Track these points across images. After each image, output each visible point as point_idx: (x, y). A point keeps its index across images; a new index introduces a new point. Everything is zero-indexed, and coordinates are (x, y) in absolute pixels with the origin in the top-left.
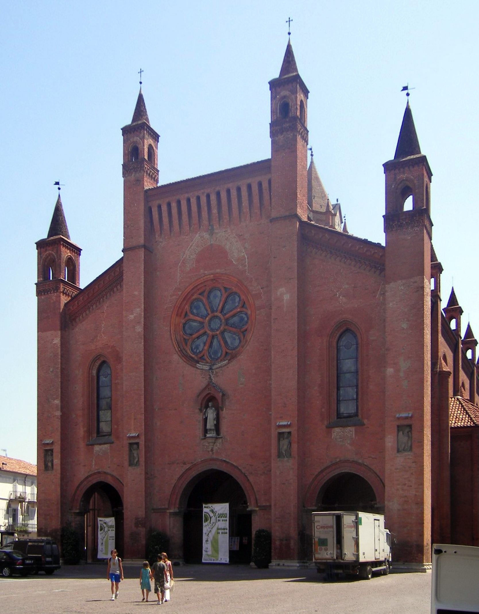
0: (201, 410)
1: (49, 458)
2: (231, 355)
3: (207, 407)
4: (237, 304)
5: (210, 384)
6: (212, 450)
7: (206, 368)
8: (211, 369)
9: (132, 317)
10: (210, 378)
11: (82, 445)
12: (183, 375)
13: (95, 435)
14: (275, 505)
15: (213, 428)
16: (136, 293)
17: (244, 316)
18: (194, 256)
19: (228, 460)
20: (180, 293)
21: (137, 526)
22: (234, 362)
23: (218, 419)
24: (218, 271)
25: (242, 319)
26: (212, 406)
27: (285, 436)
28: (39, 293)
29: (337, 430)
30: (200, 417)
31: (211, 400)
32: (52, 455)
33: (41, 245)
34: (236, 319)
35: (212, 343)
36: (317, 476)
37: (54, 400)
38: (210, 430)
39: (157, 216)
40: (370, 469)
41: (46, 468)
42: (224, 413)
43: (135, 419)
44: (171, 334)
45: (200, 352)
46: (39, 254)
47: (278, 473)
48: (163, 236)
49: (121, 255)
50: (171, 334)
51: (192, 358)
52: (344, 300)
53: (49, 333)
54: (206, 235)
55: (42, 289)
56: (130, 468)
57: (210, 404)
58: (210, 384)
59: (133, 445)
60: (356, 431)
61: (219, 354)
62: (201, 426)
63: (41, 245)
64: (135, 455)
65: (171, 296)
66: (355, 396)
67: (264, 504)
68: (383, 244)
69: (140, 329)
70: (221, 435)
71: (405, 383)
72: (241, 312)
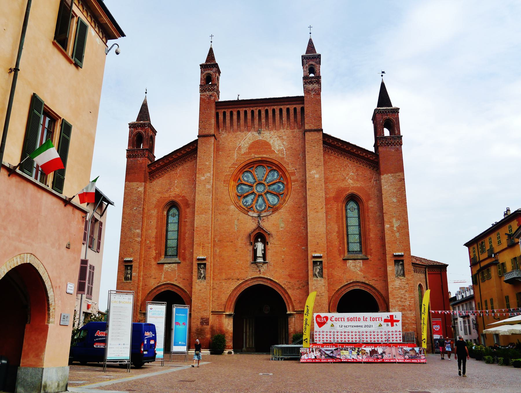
0: (251, 244)
1: (129, 272)
2: (274, 209)
3: (256, 241)
5: (259, 227)
6: (260, 271)
7: (255, 215)
8: (259, 216)
9: (203, 178)
10: (259, 222)
11: (153, 263)
12: (238, 220)
13: (163, 256)
15: (261, 256)
16: (207, 163)
18: (247, 145)
19: (272, 279)
21: (202, 323)
22: (276, 213)
23: (265, 250)
24: (265, 156)
25: (279, 187)
26: (261, 241)
28: (128, 157)
29: (351, 261)
30: (251, 248)
31: (260, 235)
32: (131, 269)
33: (132, 126)
34: (275, 186)
35: (258, 200)
36: (338, 291)
38: (260, 257)
39: (222, 118)
40: (374, 288)
41: (126, 279)
42: (269, 246)
43: (203, 247)
44: (229, 192)
47: (314, 288)
48: (224, 131)
49: (197, 138)
50: (229, 192)
51: (244, 209)
52: (351, 181)
53: (134, 184)
54: (256, 134)
55: (130, 154)
56: (198, 281)
57: (259, 240)
58: (259, 227)
59: (202, 264)
60: (363, 263)
61: (263, 208)
62: (251, 254)
63: (132, 126)
64: (202, 272)
67: (300, 310)
68: (374, 152)
69: (209, 186)
71: (397, 234)
72: (279, 182)
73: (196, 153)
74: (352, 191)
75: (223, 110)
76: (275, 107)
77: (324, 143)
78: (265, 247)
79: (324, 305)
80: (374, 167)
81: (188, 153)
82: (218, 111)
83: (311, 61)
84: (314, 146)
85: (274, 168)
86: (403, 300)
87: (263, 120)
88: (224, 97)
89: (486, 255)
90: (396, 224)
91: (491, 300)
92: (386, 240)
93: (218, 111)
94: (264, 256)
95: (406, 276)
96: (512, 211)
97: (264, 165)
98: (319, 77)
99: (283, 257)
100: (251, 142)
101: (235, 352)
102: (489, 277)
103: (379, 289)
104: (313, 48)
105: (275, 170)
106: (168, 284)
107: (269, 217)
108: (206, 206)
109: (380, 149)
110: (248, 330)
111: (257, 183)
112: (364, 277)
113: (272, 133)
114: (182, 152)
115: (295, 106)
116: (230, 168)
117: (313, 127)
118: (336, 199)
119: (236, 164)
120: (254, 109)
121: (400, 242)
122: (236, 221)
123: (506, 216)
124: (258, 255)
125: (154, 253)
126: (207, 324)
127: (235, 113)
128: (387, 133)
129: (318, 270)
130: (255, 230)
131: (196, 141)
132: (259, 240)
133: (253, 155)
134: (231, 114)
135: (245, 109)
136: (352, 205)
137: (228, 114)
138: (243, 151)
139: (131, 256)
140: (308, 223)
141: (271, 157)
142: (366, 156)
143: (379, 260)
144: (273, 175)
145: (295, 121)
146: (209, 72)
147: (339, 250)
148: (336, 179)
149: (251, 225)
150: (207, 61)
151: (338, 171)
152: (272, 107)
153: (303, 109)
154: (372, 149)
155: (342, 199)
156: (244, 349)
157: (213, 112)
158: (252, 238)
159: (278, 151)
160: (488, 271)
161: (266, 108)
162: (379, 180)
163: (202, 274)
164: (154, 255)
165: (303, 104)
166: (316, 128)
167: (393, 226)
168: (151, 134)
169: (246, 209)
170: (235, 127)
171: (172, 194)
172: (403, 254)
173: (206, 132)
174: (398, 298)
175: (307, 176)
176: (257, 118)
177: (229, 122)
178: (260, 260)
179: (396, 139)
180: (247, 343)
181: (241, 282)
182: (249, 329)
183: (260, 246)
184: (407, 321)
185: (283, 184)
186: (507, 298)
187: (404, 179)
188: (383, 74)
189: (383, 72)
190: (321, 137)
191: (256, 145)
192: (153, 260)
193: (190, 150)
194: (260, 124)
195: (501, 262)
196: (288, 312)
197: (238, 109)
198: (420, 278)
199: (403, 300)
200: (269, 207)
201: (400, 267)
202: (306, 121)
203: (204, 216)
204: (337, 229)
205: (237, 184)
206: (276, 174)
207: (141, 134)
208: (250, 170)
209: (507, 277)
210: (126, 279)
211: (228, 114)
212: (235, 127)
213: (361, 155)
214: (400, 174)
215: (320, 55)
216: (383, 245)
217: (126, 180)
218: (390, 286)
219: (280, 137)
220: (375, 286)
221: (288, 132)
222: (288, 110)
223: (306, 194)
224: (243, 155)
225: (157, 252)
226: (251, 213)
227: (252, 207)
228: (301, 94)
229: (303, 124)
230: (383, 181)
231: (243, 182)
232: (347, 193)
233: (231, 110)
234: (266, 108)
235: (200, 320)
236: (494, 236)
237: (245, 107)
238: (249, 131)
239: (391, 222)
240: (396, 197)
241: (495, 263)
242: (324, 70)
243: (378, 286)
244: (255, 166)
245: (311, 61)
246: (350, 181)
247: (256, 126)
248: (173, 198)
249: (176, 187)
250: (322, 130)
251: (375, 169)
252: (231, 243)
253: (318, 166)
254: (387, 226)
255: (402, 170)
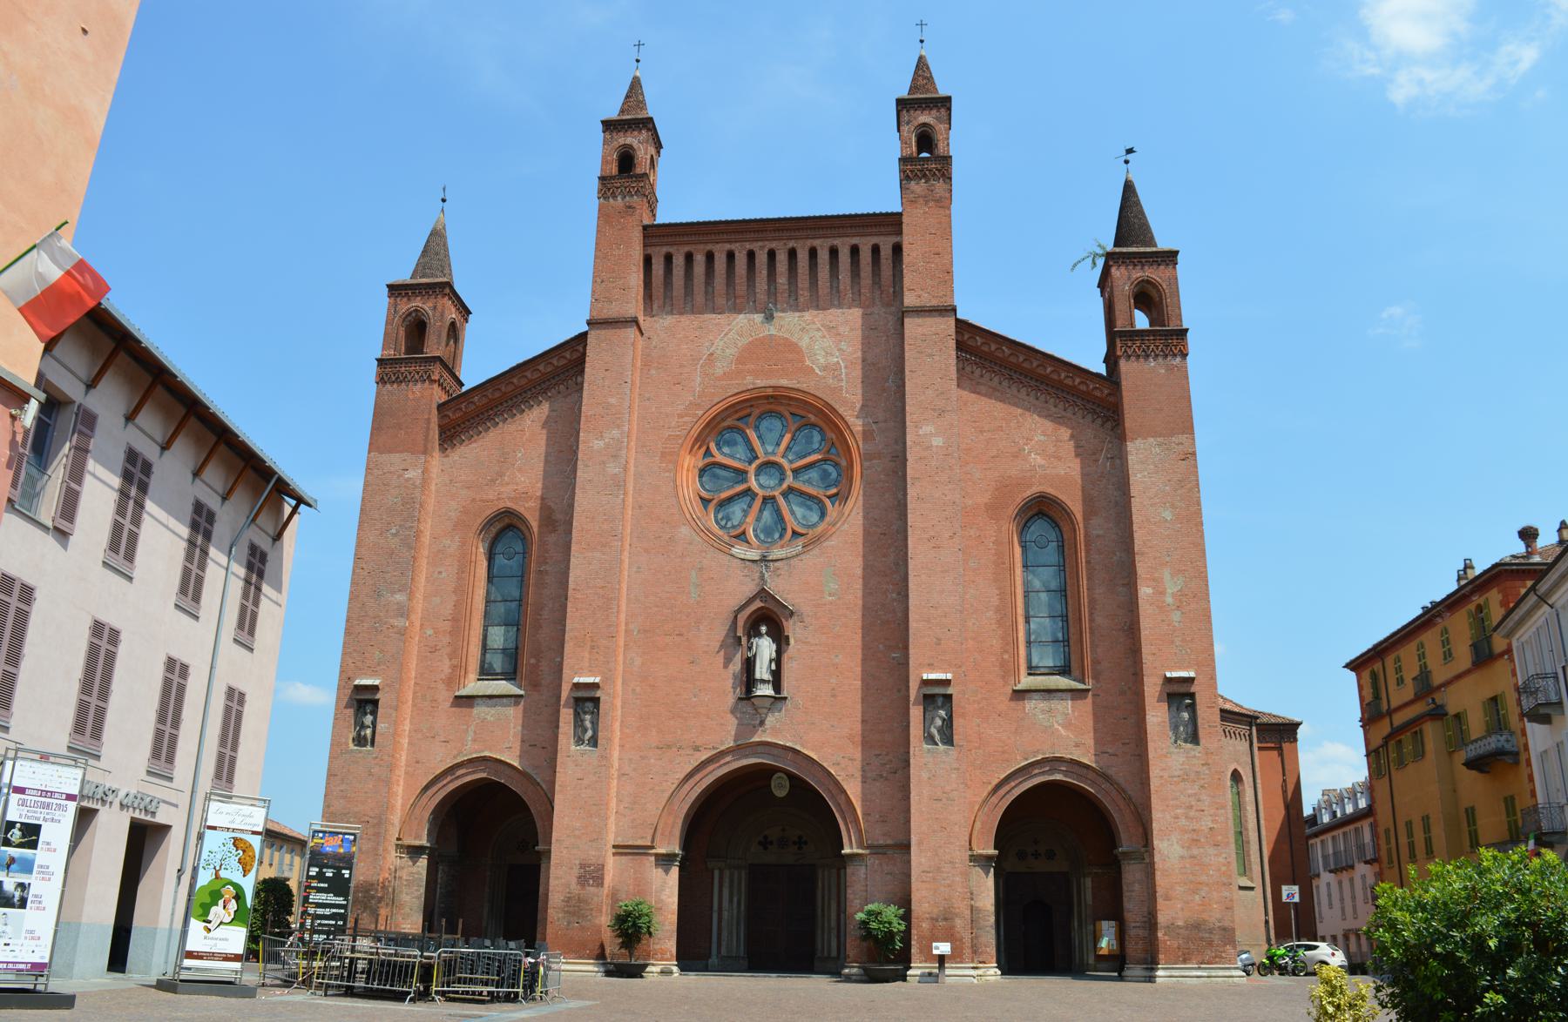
1: (368, 719)
3: (753, 631)
4: (816, 446)
5: (762, 593)
9: (598, 444)
10: (762, 577)
12: (701, 569)
14: (920, 843)
15: (767, 676)
16: (612, 401)
17: (831, 469)
18: (731, 351)
20: (700, 413)
21: (582, 880)
22: (816, 551)
23: (778, 660)
24: (784, 382)
27: (940, 701)
31: (767, 618)
32: (374, 713)
37: (393, 593)
38: (763, 681)
41: (360, 741)
43: (592, 648)
45: (733, 527)
46: (393, 309)
47: (925, 775)
49: (585, 328)
52: (1039, 460)
53: (396, 458)
57: (764, 629)
58: (762, 593)
64: (588, 724)
65: (681, 416)
66: (1060, 635)
70: (784, 694)
73: (582, 371)
74: (1041, 489)
75: (665, 250)
76: (817, 243)
77: (960, 346)
78: (779, 652)
79: (956, 829)
80: (1106, 419)
81: (557, 372)
82: (649, 251)
83: (923, 112)
84: (931, 355)
85: (812, 418)
86: (1192, 813)
87: (782, 280)
88: (669, 212)
89: (1408, 692)
90: (1172, 586)
91: (1426, 820)
92: (1145, 633)
93: (649, 251)
94: (776, 679)
95: (1202, 742)
96: (1478, 571)
97: (781, 409)
98: (947, 159)
99: (833, 681)
100: (745, 341)
101: (684, 968)
102: (1420, 754)
103: (1121, 781)
104: (930, 79)
105: (814, 426)
106: (485, 759)
107: (794, 562)
108: (605, 527)
109: (1124, 366)
110: (725, 904)
111: (758, 462)
112: (1077, 745)
113: (807, 315)
114: (541, 367)
115: (875, 240)
116: (681, 416)
117: (928, 300)
118: (993, 509)
119: (698, 406)
120: (755, 246)
121: (1184, 641)
122: (693, 573)
123: (1463, 582)
124: (758, 676)
125: (445, 667)
126: (599, 880)
127: (700, 259)
128: (1141, 321)
129: (939, 722)
130: (750, 601)
131: (582, 337)
132: (764, 629)
133: (749, 379)
134: (689, 257)
135: (728, 246)
136: (1039, 528)
137: (679, 261)
138: (720, 369)
139: (374, 674)
140: (911, 578)
141: (803, 387)
142: (1083, 388)
143: (1122, 693)
144: (809, 441)
145: (874, 283)
146: (629, 140)
147: (1003, 664)
148: (994, 452)
149: (738, 589)
150: (622, 111)
151: (1000, 428)
152: (810, 243)
153: (897, 249)
154: (1101, 369)
155: (1012, 510)
156: (714, 960)
157: (637, 253)
158: (741, 623)
159: (825, 368)
160: (1418, 738)
161: (791, 244)
162: (1120, 458)
163: (586, 730)
164: (447, 670)
165: (900, 233)
166: (934, 303)
167: (1163, 593)
168: (452, 314)
169: (726, 538)
170: (699, 298)
171: (507, 490)
172: (1192, 674)
173: (612, 311)
174: (1178, 807)
175: (909, 443)
176: (765, 272)
177: (682, 282)
178: (766, 690)
179: (1170, 339)
180: (724, 944)
181: (704, 756)
182: (731, 901)
183: (765, 648)
184: (1204, 878)
185: (836, 465)
186: (1471, 813)
187: (1194, 454)
188: (1129, 157)
189: (1130, 151)
190: (952, 330)
191: (754, 352)
192: (441, 686)
193: (563, 362)
194: (772, 292)
195: (1452, 710)
196: (846, 851)
197: (709, 247)
198: (1235, 751)
199: (1192, 813)
200: (794, 533)
201: (1186, 715)
202: (907, 282)
203: (598, 554)
204: (995, 601)
205: (701, 464)
206: (817, 437)
207: (422, 320)
208: (739, 424)
209: (1472, 751)
210: (360, 741)
211: (679, 261)
212: (699, 298)
213: (1068, 382)
214: (1183, 438)
215: (949, 99)
216: (1135, 650)
217: (373, 446)
218: (1154, 772)
219: (829, 329)
220: (1111, 772)
221: (855, 314)
222: (855, 250)
223: (905, 494)
224: (718, 379)
225: (455, 662)
226: (739, 550)
227: (744, 533)
228: (896, 207)
229: (898, 292)
230: (1132, 459)
231: (720, 458)
232: (1029, 493)
233: (687, 248)
234: (791, 244)
235: (576, 871)
236: (1430, 638)
237: (730, 242)
238: (740, 312)
239: (1157, 582)
240: (1173, 506)
241: (1438, 714)
242: (963, 141)
243: (1120, 772)
244: (756, 412)
245: (923, 112)
246: (1037, 460)
247: (761, 295)
248: (509, 504)
249: (520, 470)
250: (954, 310)
251: (1109, 425)
252: (678, 639)
253: (941, 413)
254: (1144, 591)
255: (1188, 428)
